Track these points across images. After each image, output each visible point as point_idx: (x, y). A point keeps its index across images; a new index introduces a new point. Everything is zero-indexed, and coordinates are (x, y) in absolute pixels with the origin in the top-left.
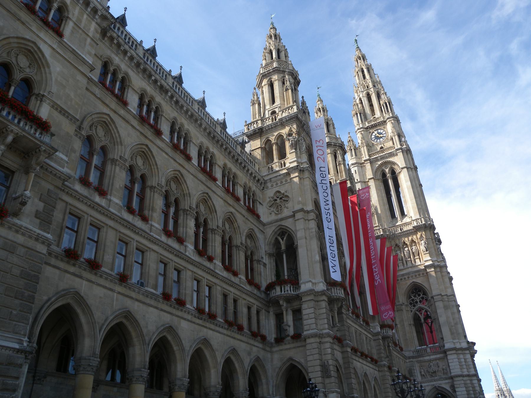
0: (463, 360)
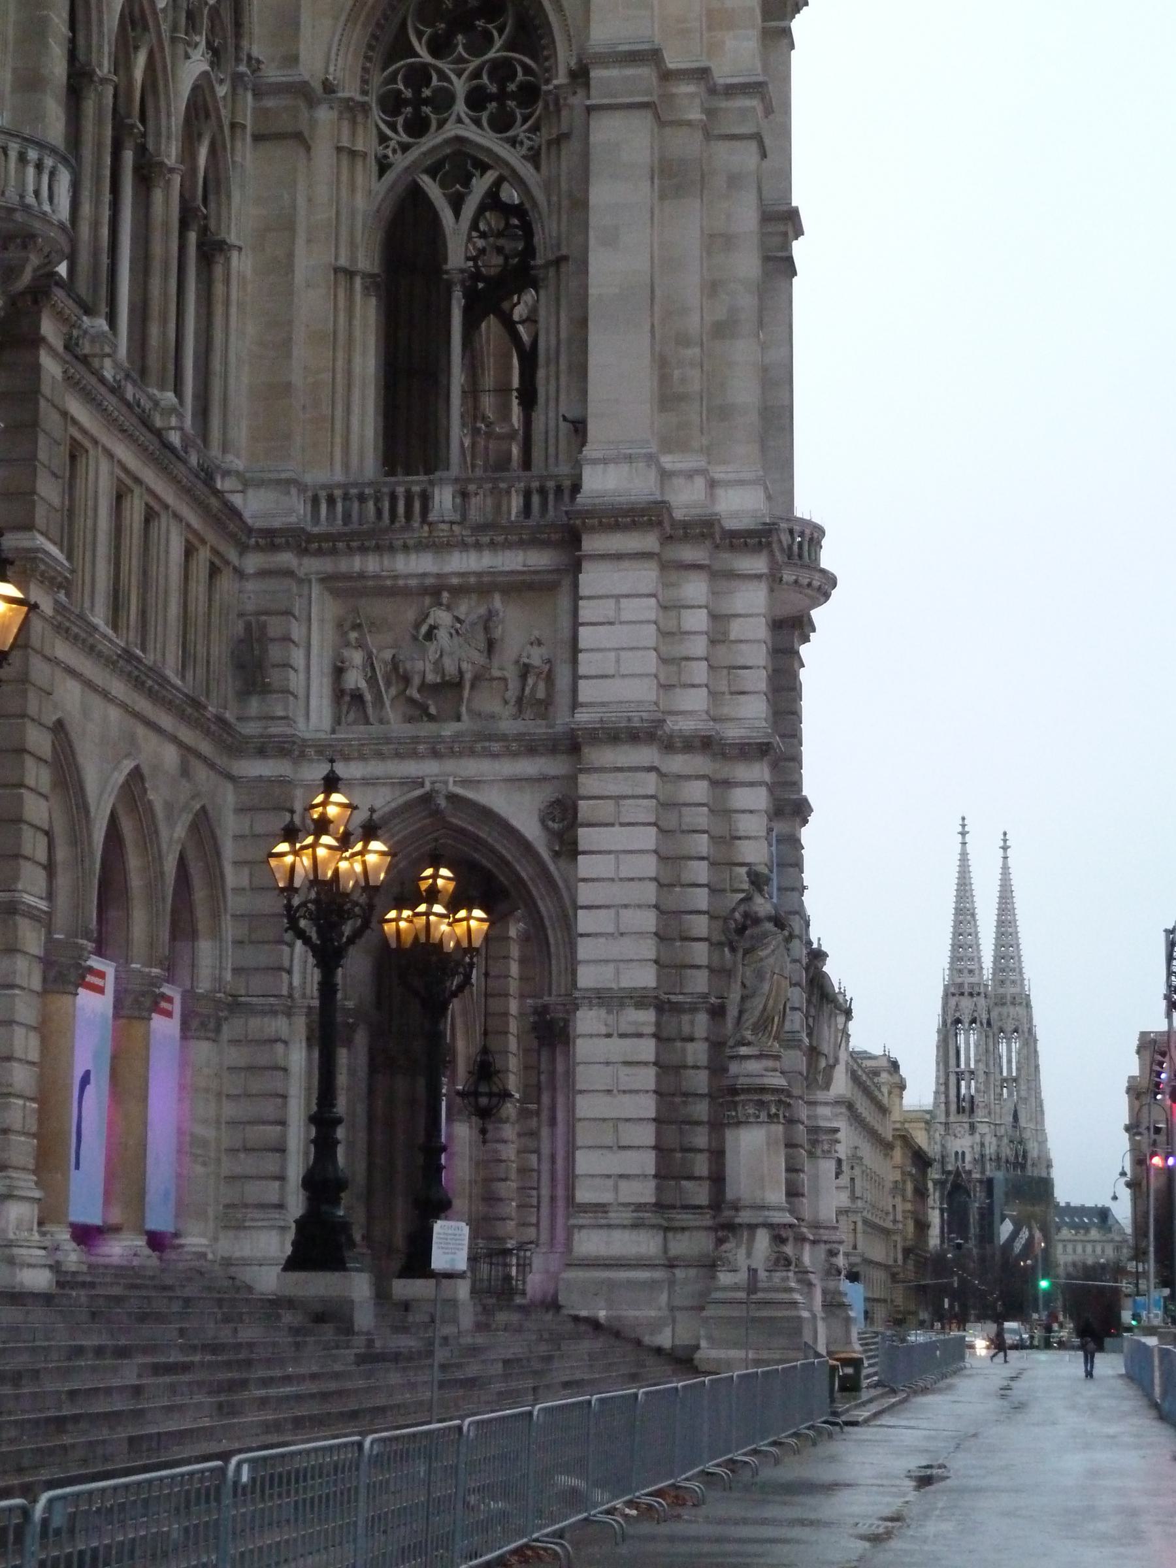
0: (697, 620)
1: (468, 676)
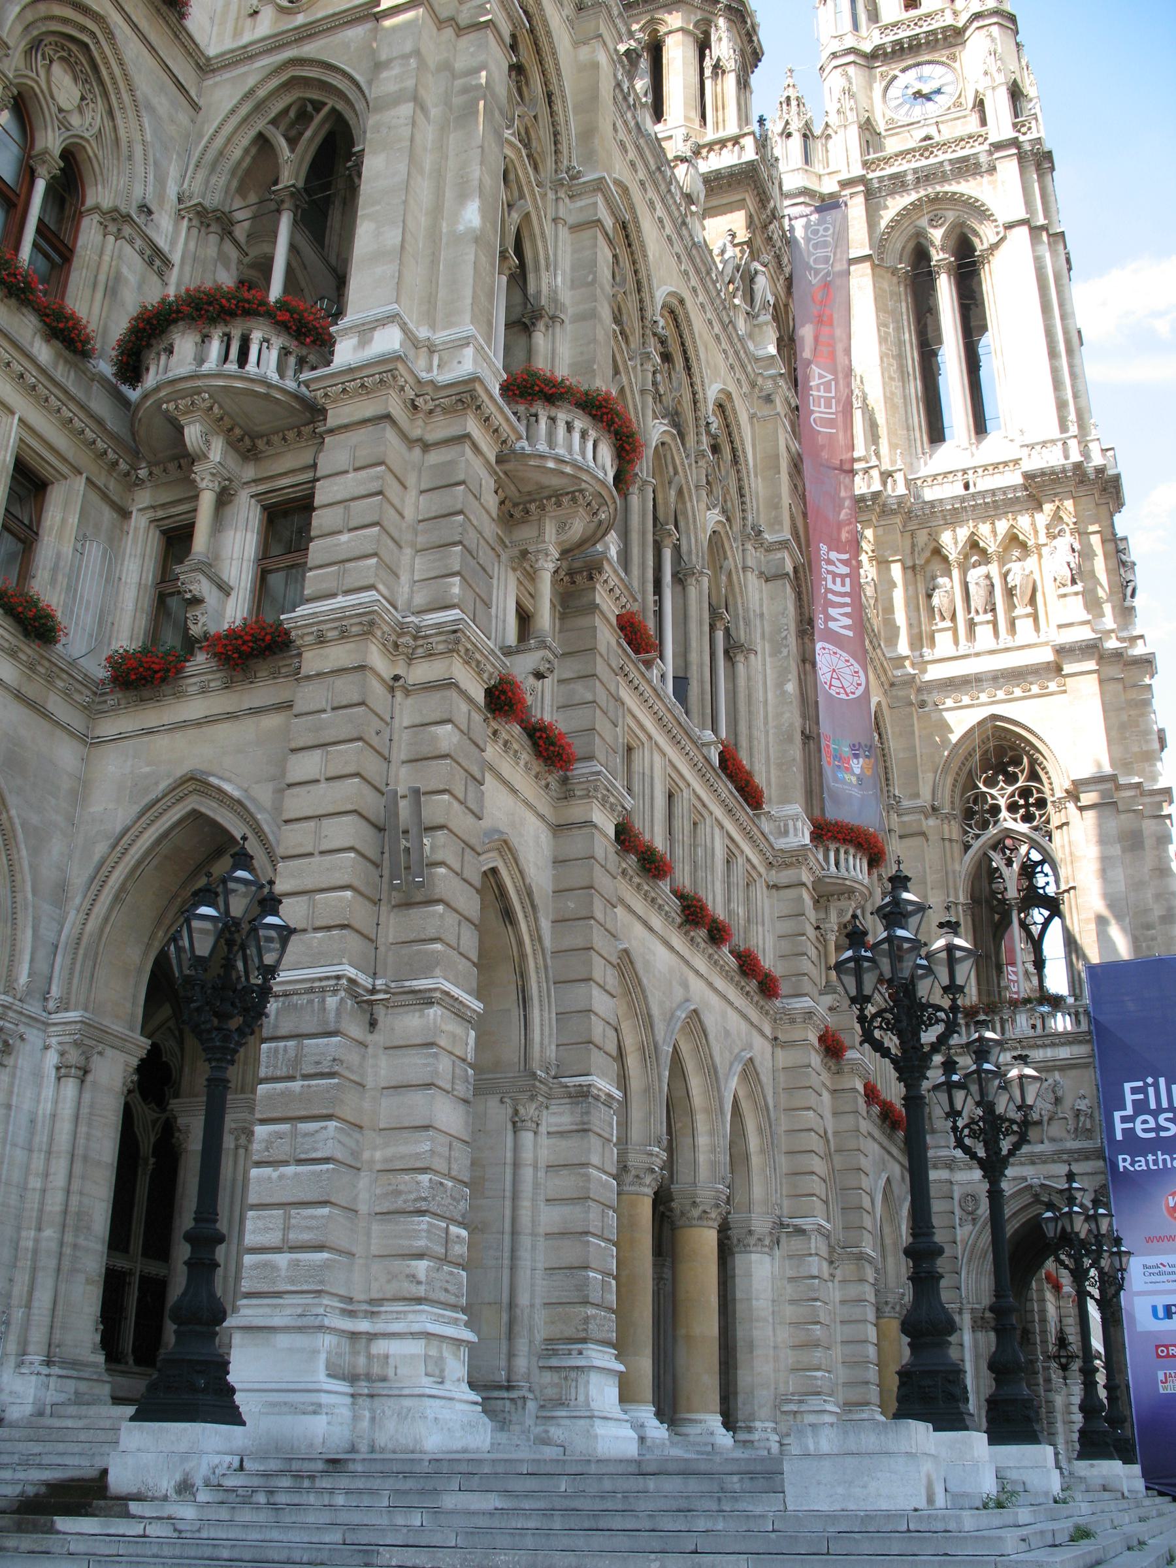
1: (1045, 1118)
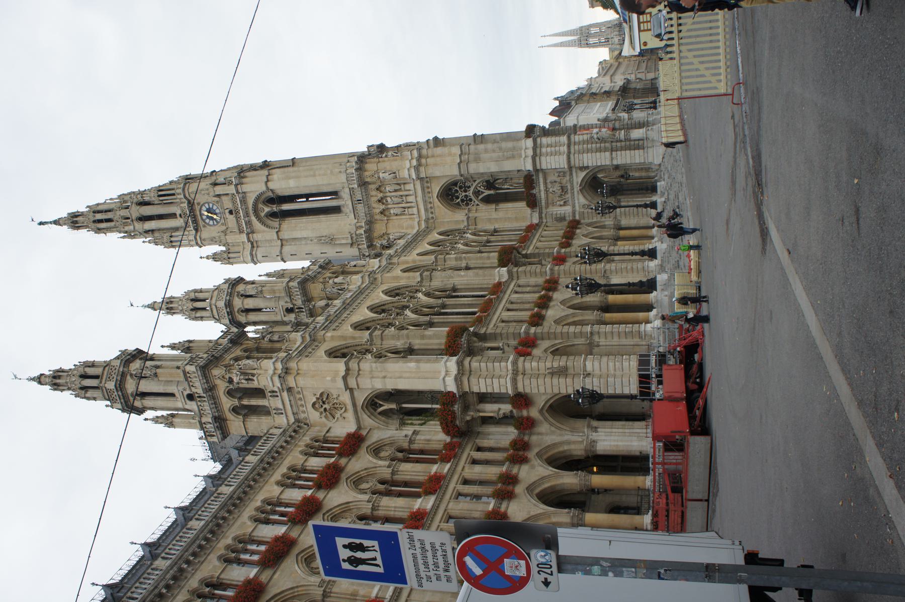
0: (549, 149)
